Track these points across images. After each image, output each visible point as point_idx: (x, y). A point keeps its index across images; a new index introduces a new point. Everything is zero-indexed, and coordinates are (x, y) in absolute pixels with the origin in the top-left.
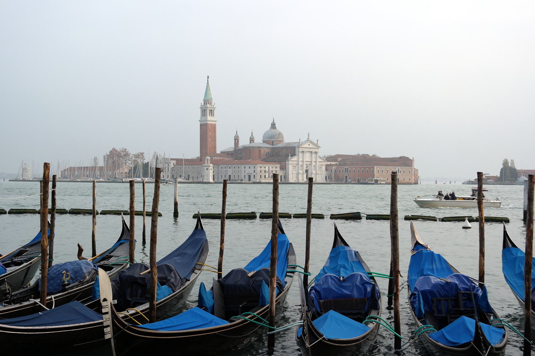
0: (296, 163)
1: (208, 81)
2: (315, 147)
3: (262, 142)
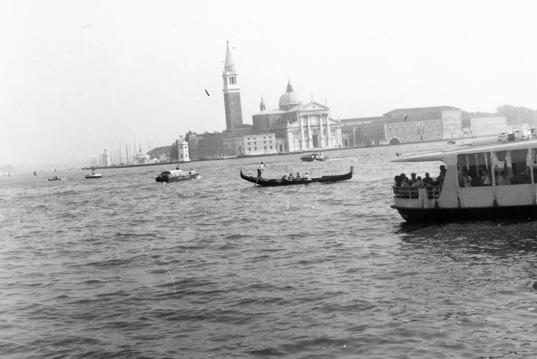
0: (298, 129)
1: (227, 46)
2: (323, 109)
3: (278, 108)
